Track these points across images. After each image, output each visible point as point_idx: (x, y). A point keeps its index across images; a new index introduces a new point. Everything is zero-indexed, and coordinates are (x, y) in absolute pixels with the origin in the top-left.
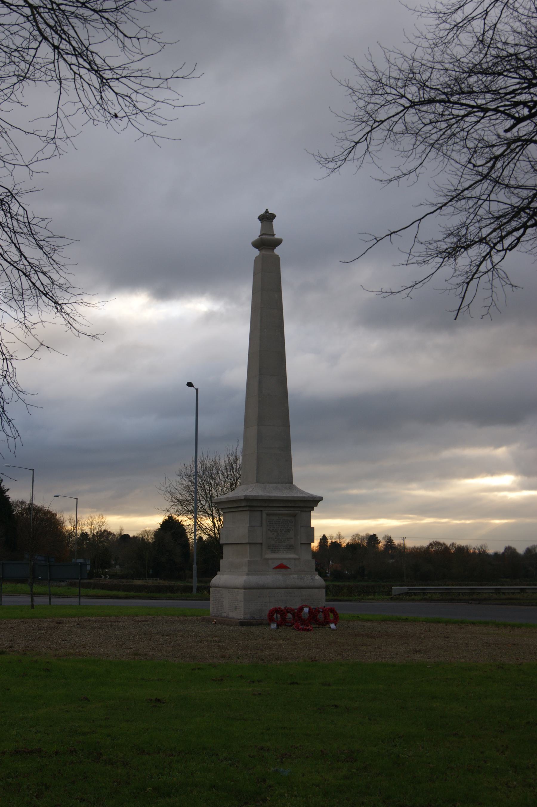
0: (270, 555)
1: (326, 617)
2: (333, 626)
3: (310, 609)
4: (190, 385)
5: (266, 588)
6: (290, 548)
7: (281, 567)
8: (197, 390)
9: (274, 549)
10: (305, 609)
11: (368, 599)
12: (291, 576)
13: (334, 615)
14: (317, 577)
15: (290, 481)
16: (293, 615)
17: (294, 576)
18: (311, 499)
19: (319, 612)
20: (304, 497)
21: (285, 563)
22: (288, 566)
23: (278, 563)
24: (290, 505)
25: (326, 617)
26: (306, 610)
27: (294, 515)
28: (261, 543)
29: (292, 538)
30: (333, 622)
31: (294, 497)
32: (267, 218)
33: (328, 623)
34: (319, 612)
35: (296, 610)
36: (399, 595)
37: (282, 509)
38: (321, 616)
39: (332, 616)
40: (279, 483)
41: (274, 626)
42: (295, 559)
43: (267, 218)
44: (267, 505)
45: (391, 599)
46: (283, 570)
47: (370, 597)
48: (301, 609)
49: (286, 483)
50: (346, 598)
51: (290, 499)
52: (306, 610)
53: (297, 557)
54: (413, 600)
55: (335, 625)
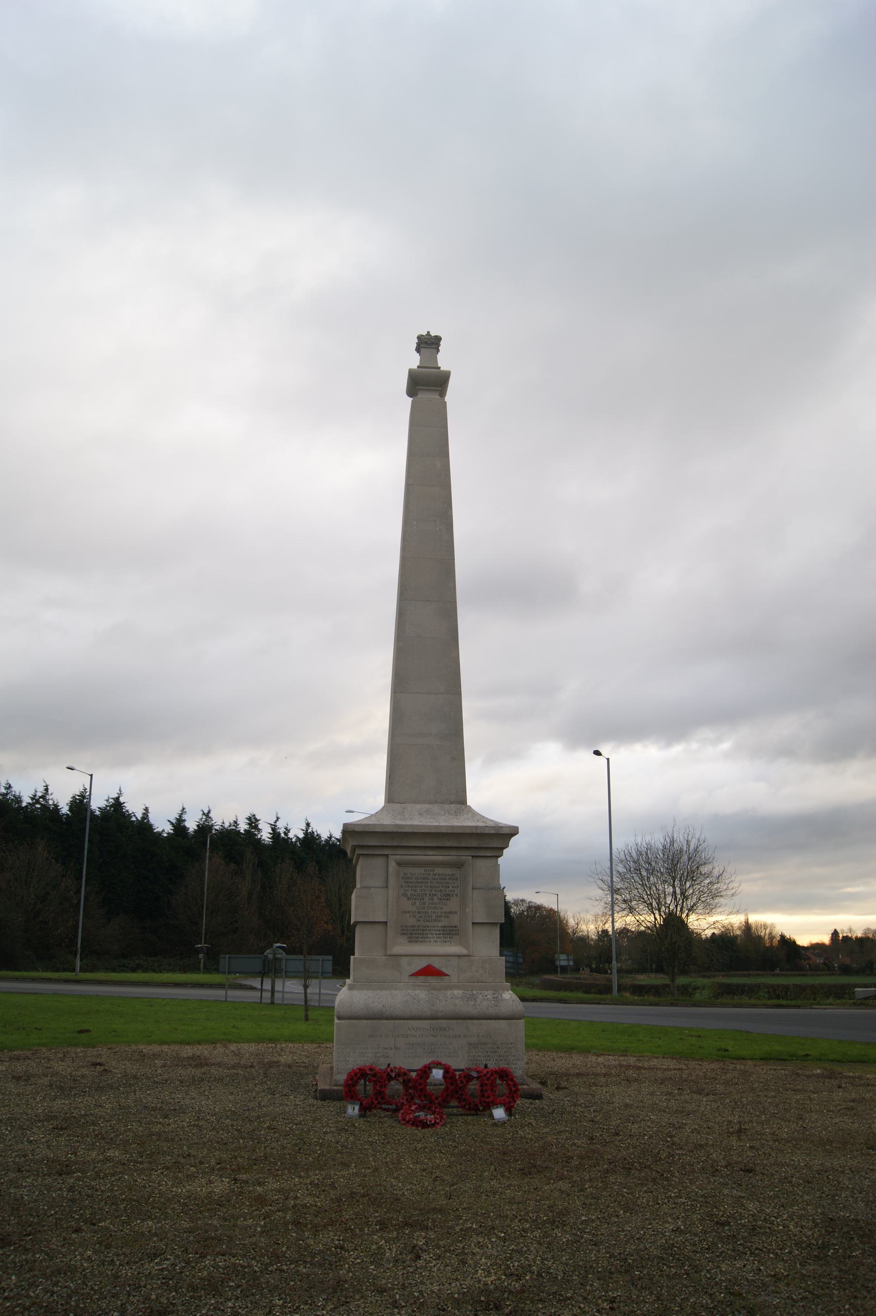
0: (402, 947)
2: (499, 1113)
3: (447, 1070)
5: (388, 1018)
6: (451, 933)
7: (429, 971)
8: (608, 759)
9: (414, 934)
10: (434, 1071)
11: (826, 1004)
12: (449, 992)
14: (509, 995)
15: (461, 800)
16: (405, 1083)
17: (456, 992)
18: (493, 832)
19: (469, 1078)
20: (476, 827)
21: (437, 964)
23: (422, 964)
24: (448, 844)
26: (437, 1074)
27: (459, 865)
29: (455, 913)
31: (453, 827)
32: (428, 344)
33: (488, 1106)
34: (469, 1078)
35: (414, 1074)
36: (865, 999)
37: (436, 852)
39: (502, 1087)
40: (436, 802)
41: (353, 1110)
42: (459, 956)
43: (428, 344)
44: (395, 844)
45: (854, 1004)
46: (433, 980)
47: (828, 1001)
48: (425, 1072)
49: (452, 803)
50: (793, 1003)
51: (443, 831)
52: (437, 1074)
55: (509, 1111)
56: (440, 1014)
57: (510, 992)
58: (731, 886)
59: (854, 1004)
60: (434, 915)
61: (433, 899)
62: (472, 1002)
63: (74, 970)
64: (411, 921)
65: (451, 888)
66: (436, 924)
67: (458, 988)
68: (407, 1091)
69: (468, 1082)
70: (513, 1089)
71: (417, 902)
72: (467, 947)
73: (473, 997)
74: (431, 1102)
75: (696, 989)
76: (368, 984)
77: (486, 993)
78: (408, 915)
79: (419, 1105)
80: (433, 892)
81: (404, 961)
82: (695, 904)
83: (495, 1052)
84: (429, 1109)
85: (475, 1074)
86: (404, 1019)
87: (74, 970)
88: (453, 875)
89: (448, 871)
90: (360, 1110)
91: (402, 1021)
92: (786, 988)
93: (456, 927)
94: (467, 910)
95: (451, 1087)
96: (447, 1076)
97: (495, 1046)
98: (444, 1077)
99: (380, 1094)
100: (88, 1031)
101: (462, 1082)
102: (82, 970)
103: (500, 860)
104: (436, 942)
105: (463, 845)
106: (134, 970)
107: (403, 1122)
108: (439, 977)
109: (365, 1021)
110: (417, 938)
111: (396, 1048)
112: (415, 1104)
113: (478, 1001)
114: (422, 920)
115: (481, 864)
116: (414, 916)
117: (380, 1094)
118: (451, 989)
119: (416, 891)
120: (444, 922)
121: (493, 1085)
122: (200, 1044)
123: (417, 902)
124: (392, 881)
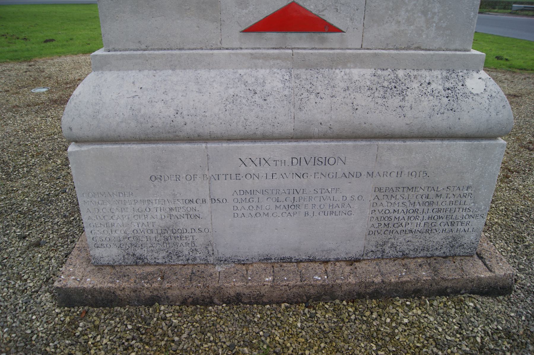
5: (190, 140)
12: (339, 74)
17: (356, 72)
36: (517, 10)
45: (510, 13)
46: (301, 43)
54: (527, 15)
56: (316, 130)
57: (483, 74)
59: (510, 13)
62: (396, 101)
67: (360, 61)
73: (397, 88)
83: (430, 204)
86: (229, 140)
91: (225, 145)
100: (52, 40)
108: (317, 36)
109: (135, 147)
111: (213, 200)
113: (410, 97)
118: (345, 66)
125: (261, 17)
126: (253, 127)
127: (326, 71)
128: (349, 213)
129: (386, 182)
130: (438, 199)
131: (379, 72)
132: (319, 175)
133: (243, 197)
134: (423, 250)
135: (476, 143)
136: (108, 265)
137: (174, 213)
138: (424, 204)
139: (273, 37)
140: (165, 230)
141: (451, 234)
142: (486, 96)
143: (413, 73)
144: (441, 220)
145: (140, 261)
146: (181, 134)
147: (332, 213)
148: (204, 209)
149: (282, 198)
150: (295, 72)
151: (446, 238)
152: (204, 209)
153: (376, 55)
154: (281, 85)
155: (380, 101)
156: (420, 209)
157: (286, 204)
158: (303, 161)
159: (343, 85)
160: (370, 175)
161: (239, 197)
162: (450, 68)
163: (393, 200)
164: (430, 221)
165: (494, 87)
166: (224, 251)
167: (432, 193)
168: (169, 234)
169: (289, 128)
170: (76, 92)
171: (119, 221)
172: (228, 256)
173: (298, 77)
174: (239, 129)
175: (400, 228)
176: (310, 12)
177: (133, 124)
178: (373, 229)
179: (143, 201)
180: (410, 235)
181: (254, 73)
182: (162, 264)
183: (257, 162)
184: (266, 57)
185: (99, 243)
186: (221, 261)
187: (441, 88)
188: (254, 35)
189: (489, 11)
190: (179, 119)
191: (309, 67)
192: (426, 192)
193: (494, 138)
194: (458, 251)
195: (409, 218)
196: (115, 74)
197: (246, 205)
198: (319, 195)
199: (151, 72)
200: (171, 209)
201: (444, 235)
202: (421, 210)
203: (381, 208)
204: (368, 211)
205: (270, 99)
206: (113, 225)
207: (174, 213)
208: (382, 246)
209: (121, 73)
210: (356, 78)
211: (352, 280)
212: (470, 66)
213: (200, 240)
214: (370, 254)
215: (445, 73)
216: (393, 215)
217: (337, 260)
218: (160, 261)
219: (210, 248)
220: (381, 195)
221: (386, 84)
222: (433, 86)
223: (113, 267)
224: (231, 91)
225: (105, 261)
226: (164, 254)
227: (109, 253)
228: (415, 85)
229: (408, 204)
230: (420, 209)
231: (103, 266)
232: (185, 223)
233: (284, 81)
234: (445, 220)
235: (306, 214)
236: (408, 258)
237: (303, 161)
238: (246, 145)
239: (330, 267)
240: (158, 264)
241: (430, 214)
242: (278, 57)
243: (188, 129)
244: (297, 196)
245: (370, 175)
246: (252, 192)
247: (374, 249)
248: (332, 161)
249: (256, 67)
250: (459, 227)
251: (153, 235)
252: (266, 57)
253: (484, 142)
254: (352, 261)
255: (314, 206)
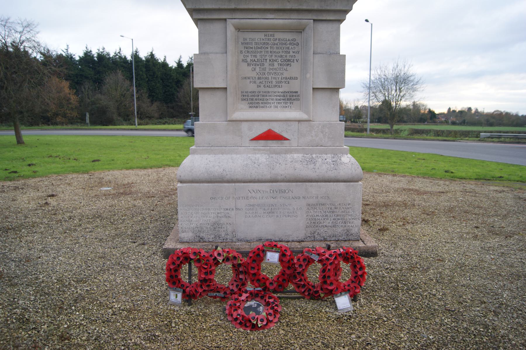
0: (244, 113)
1: (329, 271)
2: (343, 302)
3: (283, 255)
4: (367, 21)
5: (228, 182)
6: (291, 98)
7: (269, 136)
9: (254, 100)
12: (289, 156)
13: (354, 266)
14: (347, 159)
17: (295, 156)
19: (310, 261)
21: (277, 129)
22: (285, 135)
23: (262, 129)
25: (329, 271)
26: (273, 257)
28: (226, 88)
29: (296, 78)
30: (344, 290)
33: (332, 293)
34: (310, 261)
38: (313, 274)
42: (299, 121)
44: (233, 6)
45: (479, 140)
46: (273, 144)
48: (258, 255)
52: (273, 257)
53: (305, 116)
54: (493, 142)
55: (354, 298)
56: (279, 178)
57: (349, 155)
58: (422, 86)
59: (479, 140)
60: (274, 81)
61: (273, 65)
62: (312, 166)
63: (135, 125)
64: (252, 87)
65: (291, 54)
66: (276, 89)
67: (297, 151)
68: (238, 275)
69: (307, 265)
70: (360, 273)
71: (258, 68)
72: (307, 113)
73: (312, 161)
74: (265, 289)
75: (401, 131)
76: (212, 148)
77: (325, 156)
78: (248, 81)
79: (251, 293)
80: (273, 58)
81: (245, 126)
82: (405, 94)
83: (333, 212)
84: (262, 297)
85: (316, 258)
86: (244, 182)
87: (135, 125)
88: (294, 40)
89: (288, 36)
90: (183, 297)
91: (242, 184)
92: (443, 132)
93: (296, 92)
94: (308, 76)
95: (288, 272)
96: (284, 259)
97: (333, 207)
98: (281, 260)
99: (206, 282)
100: (98, 160)
101: (301, 265)
102: (139, 125)
103: (343, 26)
104: (277, 107)
105: (304, 7)
106: (164, 124)
107: (230, 318)
108: (280, 142)
109: (206, 184)
110: (258, 103)
111: (237, 209)
112: (246, 292)
113: (318, 164)
114: (262, 85)
115: (322, 27)
116: (255, 82)
117: (206, 282)
119: (256, 56)
120: (285, 88)
121: (337, 270)
122: (151, 168)
123: (258, 68)
124: (231, 47)
125: (257, 135)
126: (254, 176)
127: (283, 155)
128: (296, 216)
129: (312, 201)
130: (336, 210)
131: (305, 155)
132: (282, 198)
133: (250, 208)
134: (333, 236)
135: (348, 183)
136: (187, 242)
137: (219, 215)
138: (330, 212)
139: (262, 142)
140: (214, 223)
141: (345, 228)
142: (350, 164)
143: (319, 156)
144: (339, 221)
145: (201, 240)
146: (225, 179)
147: (289, 216)
148: (232, 213)
149: (266, 208)
150: (271, 155)
151: (344, 230)
152: (232, 213)
153: (303, 149)
154: (265, 160)
155: (305, 166)
156: (329, 214)
157: (268, 211)
158: (275, 192)
159: (290, 160)
160: (304, 198)
161: (248, 208)
162: (335, 153)
163: (316, 210)
164: (334, 221)
165: (353, 160)
166: (240, 235)
167: (333, 207)
168: (216, 225)
169: (268, 177)
170: (183, 162)
171: (195, 219)
172: (242, 238)
173: (272, 157)
174: (249, 178)
175: (321, 225)
176: (275, 132)
177: (206, 175)
178: (308, 225)
179: (206, 209)
180: (326, 228)
181: (254, 156)
182: (212, 242)
183: (256, 191)
184: (259, 150)
185: (184, 230)
186: (239, 240)
187: (331, 161)
188: (254, 141)
189: (462, 139)
190: (225, 173)
191: (277, 153)
192: (330, 206)
193: (357, 181)
194: (351, 237)
195: (324, 219)
196: (199, 156)
197: (251, 212)
198: (282, 207)
199: (214, 155)
200: (218, 213)
201: (342, 228)
202: (329, 216)
203: (310, 214)
204: (305, 216)
205: (261, 165)
206: (191, 221)
207: (219, 215)
208: (313, 234)
209: (202, 156)
210: (295, 157)
211: (299, 246)
212: (344, 152)
213: (230, 229)
214: (308, 238)
215: (333, 155)
216: (317, 218)
217: (293, 241)
218: (211, 240)
219: (234, 234)
220: (310, 208)
221: (308, 160)
222: (328, 160)
223: (188, 243)
224: (245, 163)
225: (185, 240)
226: (213, 236)
227: (187, 236)
228: (320, 160)
229: (322, 212)
230: (329, 214)
231: (184, 242)
232: (224, 220)
233: (266, 159)
234: (341, 221)
235: (277, 216)
236: (327, 241)
237: (275, 192)
238: (251, 184)
239: (289, 243)
240: (210, 242)
241: (334, 217)
242: (264, 150)
243: (228, 177)
244: (273, 208)
245: (304, 198)
246: (253, 205)
247: (310, 235)
248: (287, 191)
249: (255, 153)
250: (349, 224)
251: (209, 226)
252: (259, 150)
253: (352, 183)
254: (300, 242)
255: (280, 212)
